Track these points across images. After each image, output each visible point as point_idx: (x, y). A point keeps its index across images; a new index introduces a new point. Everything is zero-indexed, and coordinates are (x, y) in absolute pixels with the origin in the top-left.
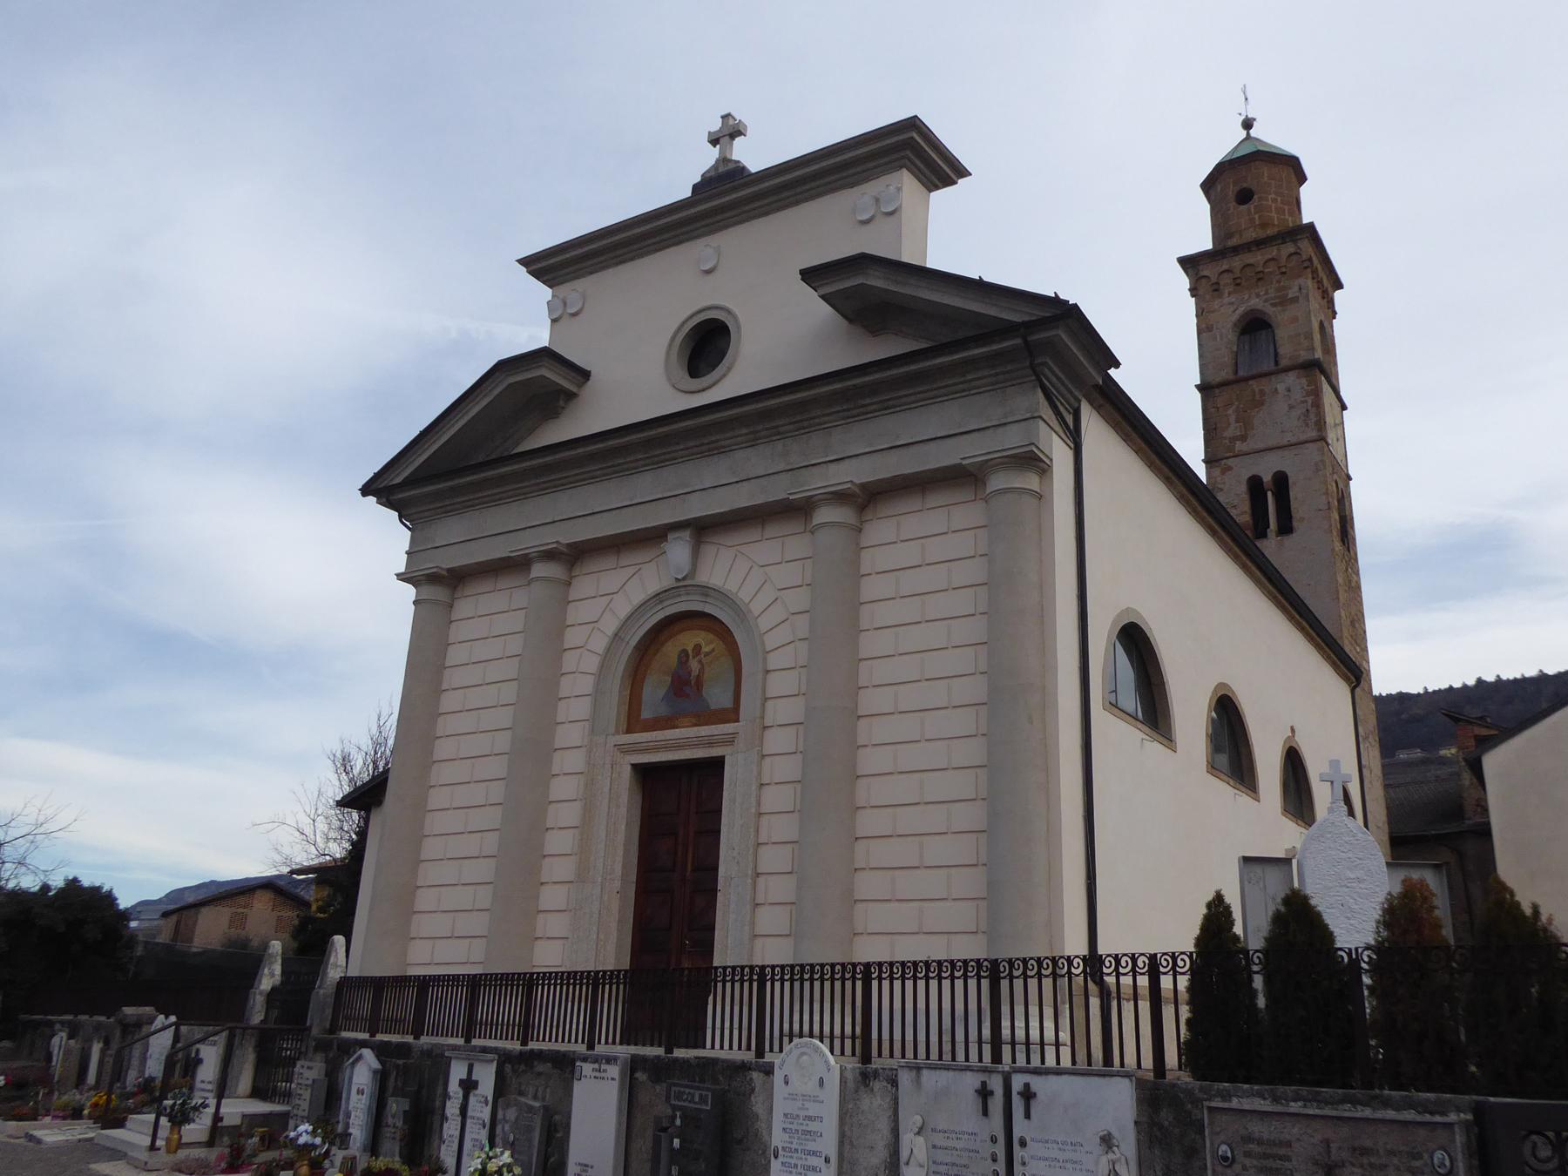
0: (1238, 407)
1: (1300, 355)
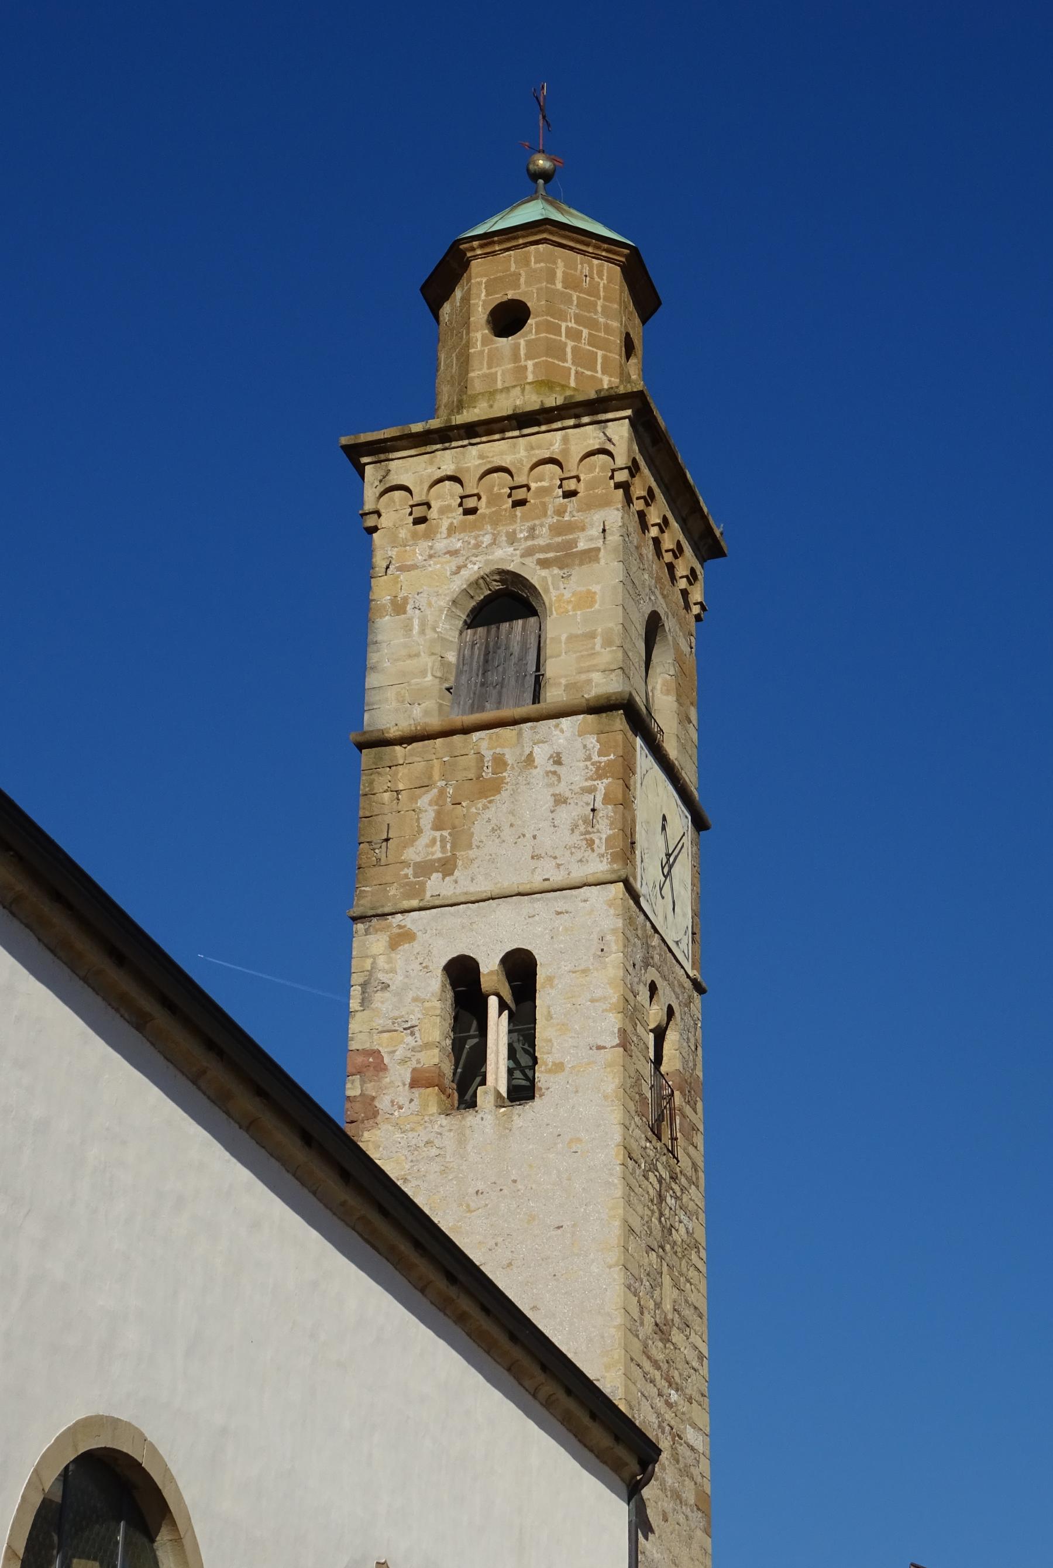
0: (442, 792)
1: (589, 681)
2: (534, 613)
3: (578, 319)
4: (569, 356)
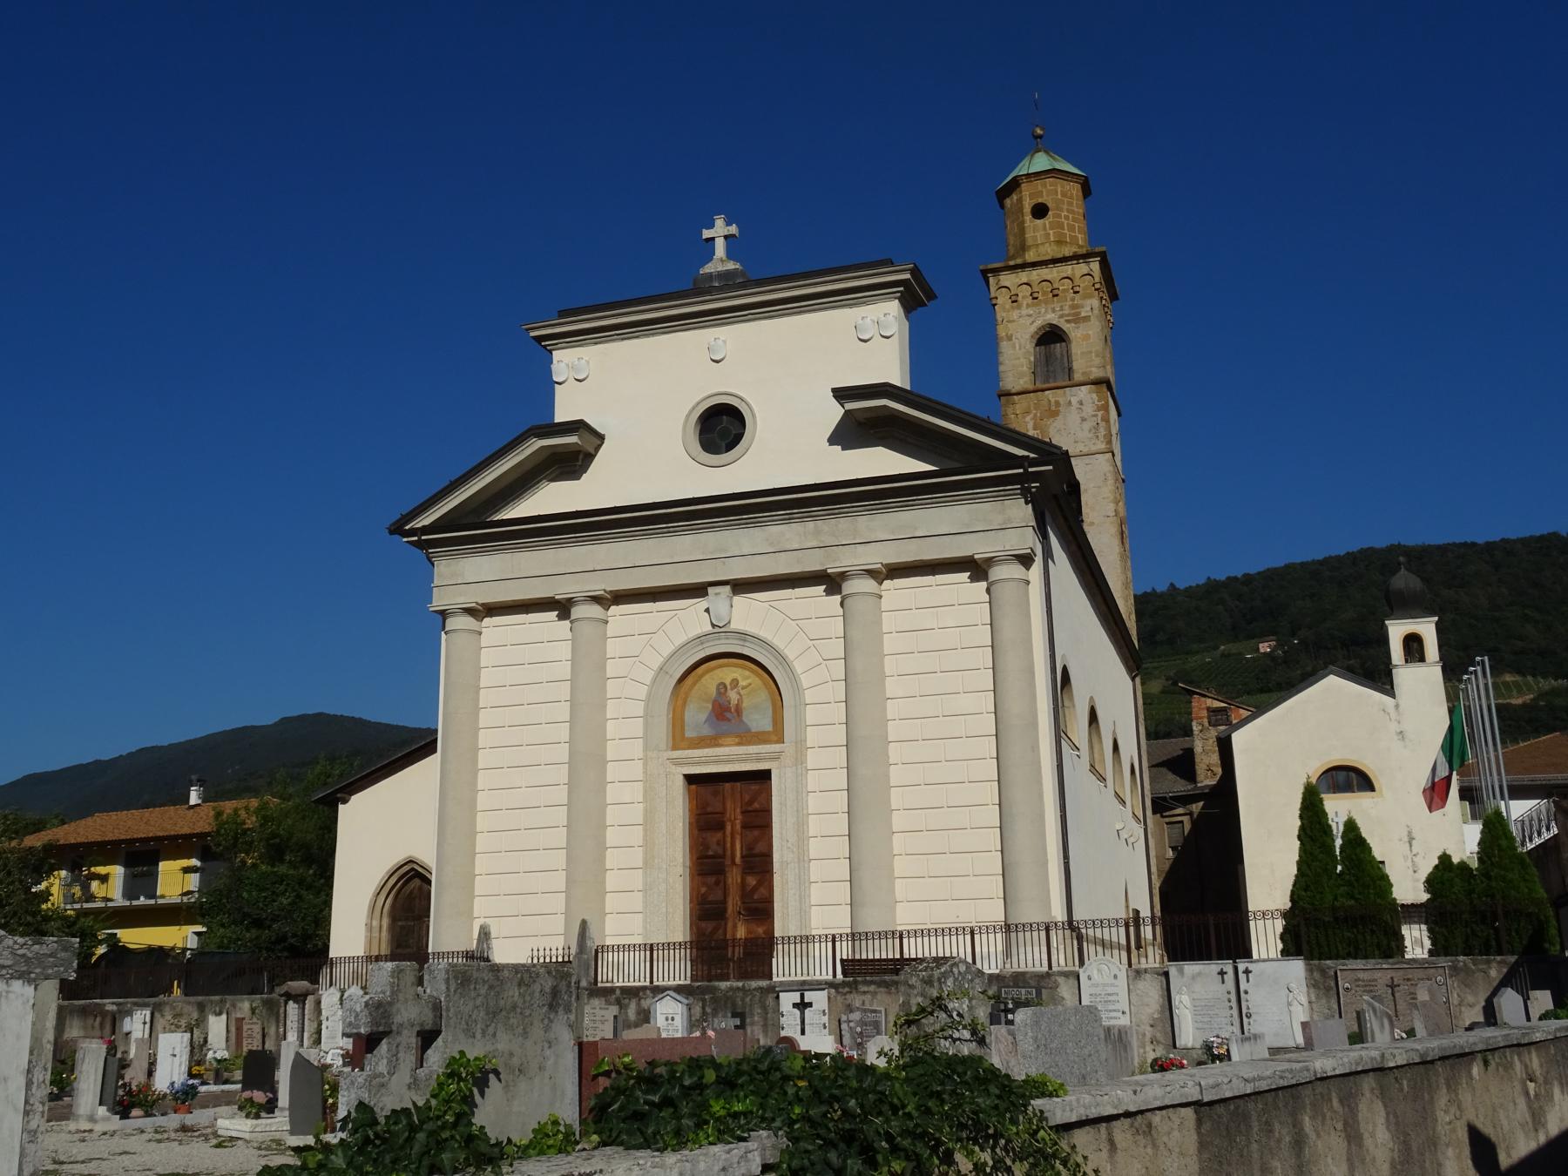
0: (1035, 415)
2: (1064, 341)
3: (1068, 211)
4: (1066, 228)
